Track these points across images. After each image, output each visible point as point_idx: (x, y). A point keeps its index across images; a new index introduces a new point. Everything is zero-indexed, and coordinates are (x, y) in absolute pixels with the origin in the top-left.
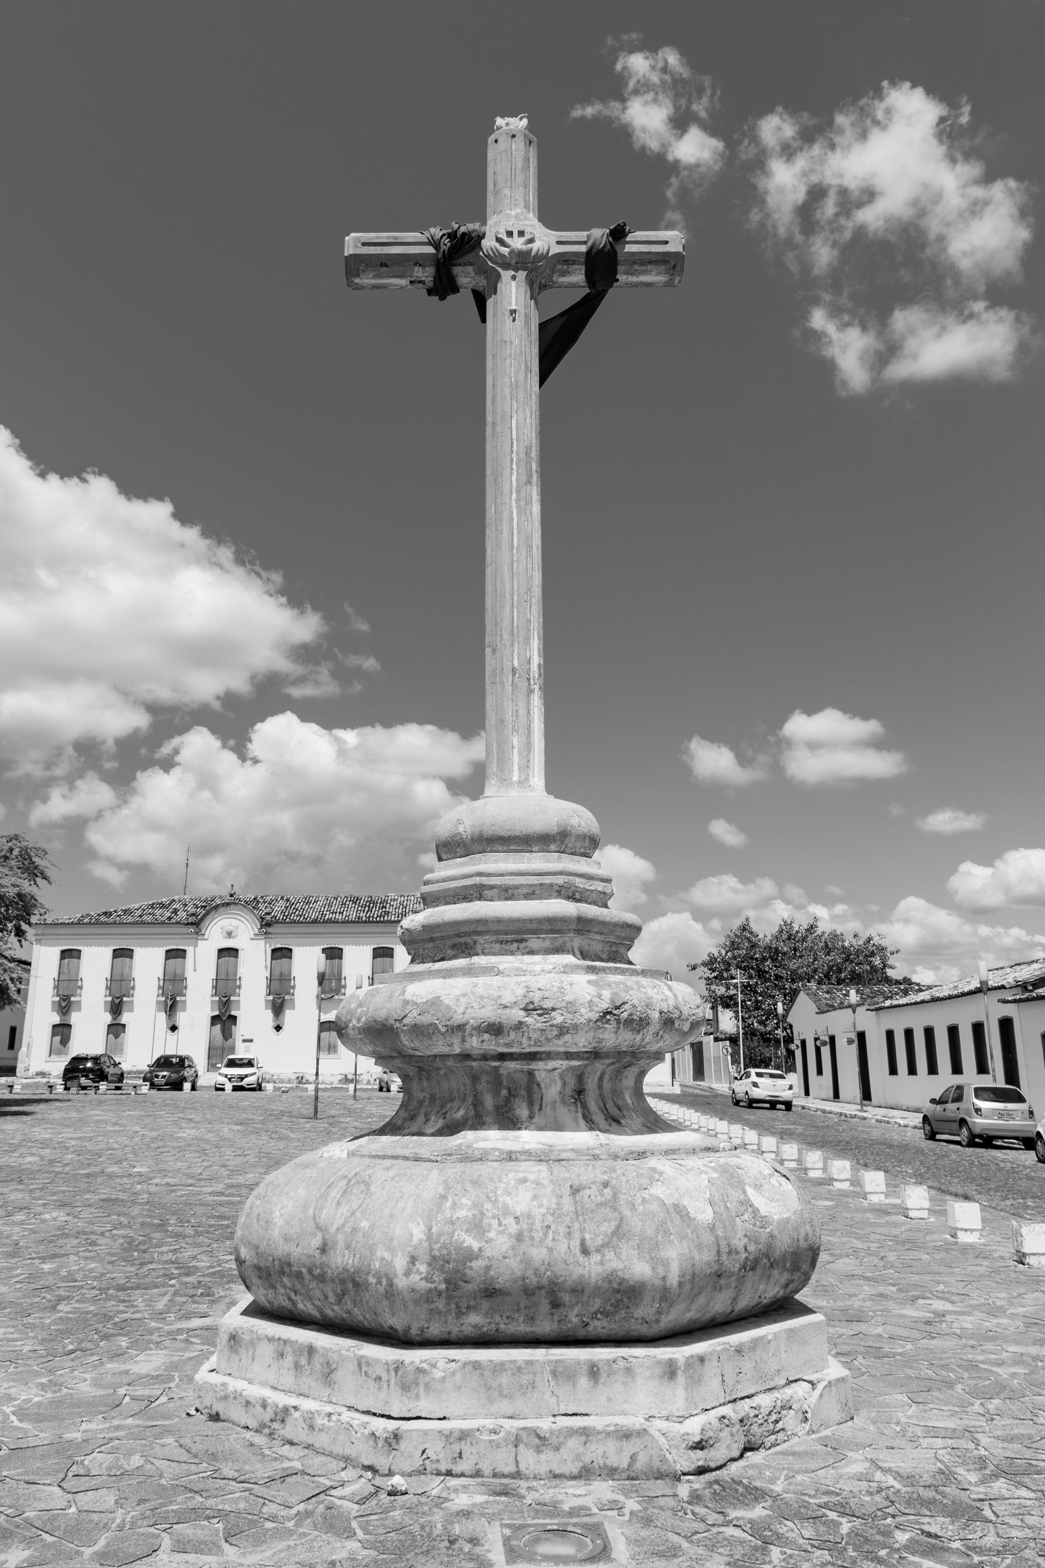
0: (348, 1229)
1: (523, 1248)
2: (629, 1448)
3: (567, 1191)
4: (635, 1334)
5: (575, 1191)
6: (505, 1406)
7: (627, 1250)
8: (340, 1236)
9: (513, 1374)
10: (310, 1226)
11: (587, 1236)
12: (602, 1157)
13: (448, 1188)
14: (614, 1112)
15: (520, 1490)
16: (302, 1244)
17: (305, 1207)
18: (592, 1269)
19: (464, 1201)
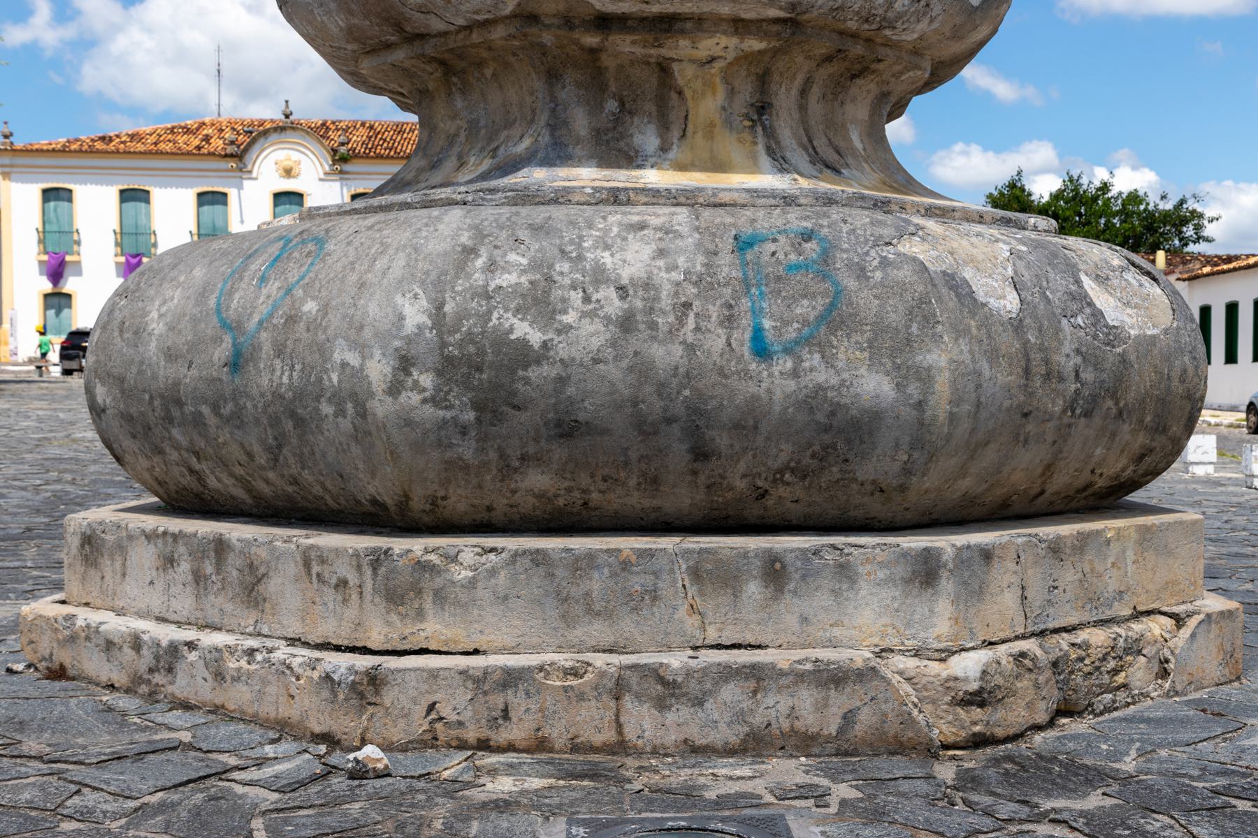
0: (278, 320)
1: (634, 343)
2: (840, 702)
3: (727, 244)
4: (859, 513)
5: (743, 244)
6: (598, 631)
7: (846, 350)
8: (264, 335)
9: (613, 575)
10: (210, 327)
11: (767, 324)
12: (802, 201)
13: (480, 235)
14: (831, 156)
15: (622, 771)
16: (197, 361)
17: (203, 294)
18: (776, 382)
19: (512, 257)
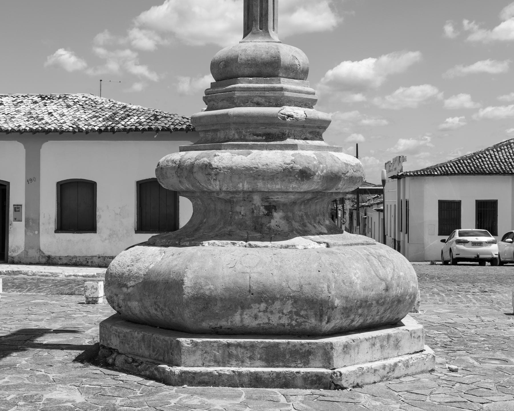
0: (396, 277)
8: (393, 281)
10: (377, 280)
16: (375, 289)
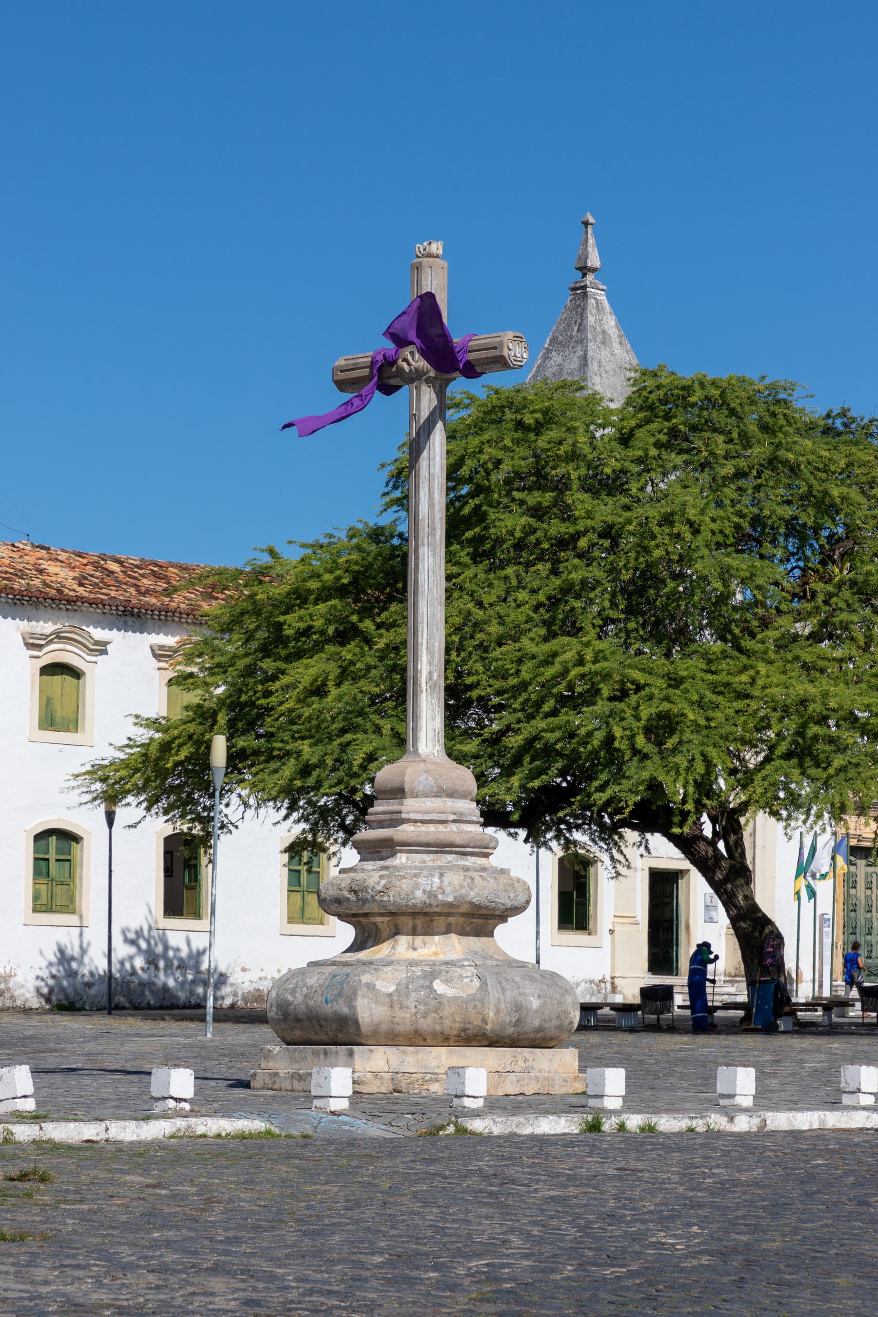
18: (328, 1009)
